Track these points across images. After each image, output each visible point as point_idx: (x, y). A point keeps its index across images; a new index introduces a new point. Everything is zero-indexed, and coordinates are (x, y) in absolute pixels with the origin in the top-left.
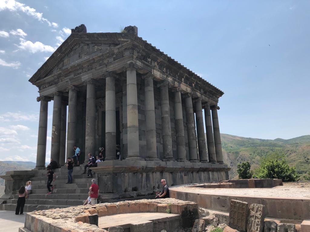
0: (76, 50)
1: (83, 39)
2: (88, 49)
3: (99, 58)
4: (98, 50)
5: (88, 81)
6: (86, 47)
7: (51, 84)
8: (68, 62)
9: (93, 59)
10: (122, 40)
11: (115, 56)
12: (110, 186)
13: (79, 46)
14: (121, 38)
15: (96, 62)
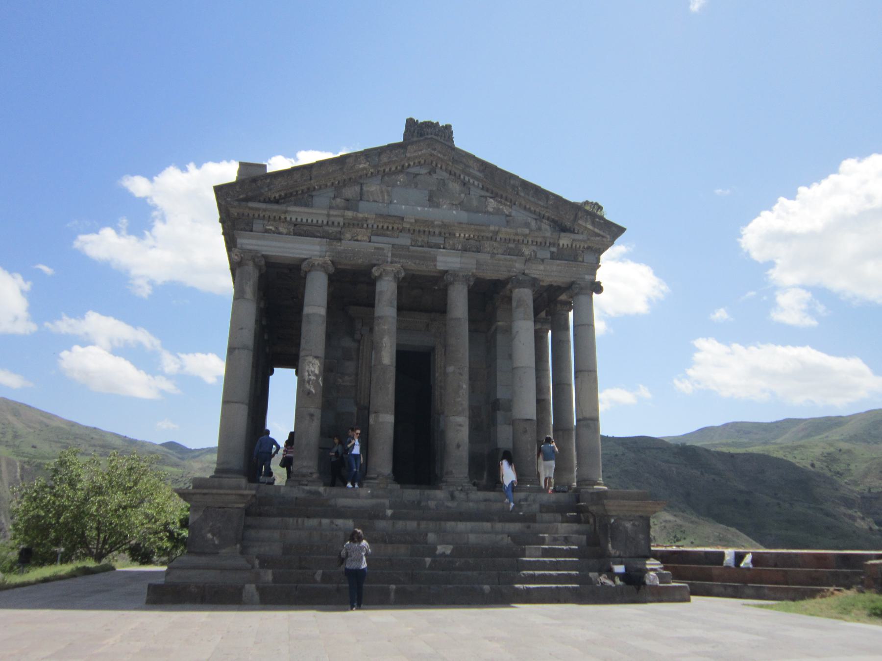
0: (419, 177)
1: (461, 167)
2: (463, 195)
3: (512, 237)
4: (498, 212)
5: (461, 274)
6: (455, 187)
7: (300, 230)
8: (383, 196)
9: (496, 233)
10: (590, 227)
11: (554, 249)
12: (643, 542)
13: (430, 173)
14: (586, 221)
15: (498, 239)
